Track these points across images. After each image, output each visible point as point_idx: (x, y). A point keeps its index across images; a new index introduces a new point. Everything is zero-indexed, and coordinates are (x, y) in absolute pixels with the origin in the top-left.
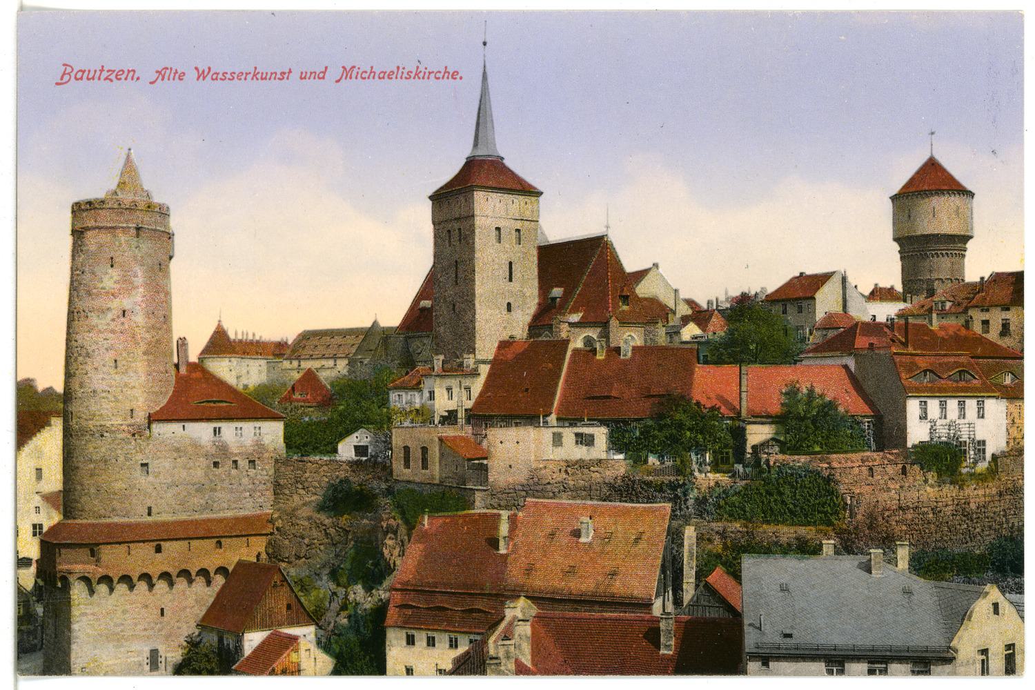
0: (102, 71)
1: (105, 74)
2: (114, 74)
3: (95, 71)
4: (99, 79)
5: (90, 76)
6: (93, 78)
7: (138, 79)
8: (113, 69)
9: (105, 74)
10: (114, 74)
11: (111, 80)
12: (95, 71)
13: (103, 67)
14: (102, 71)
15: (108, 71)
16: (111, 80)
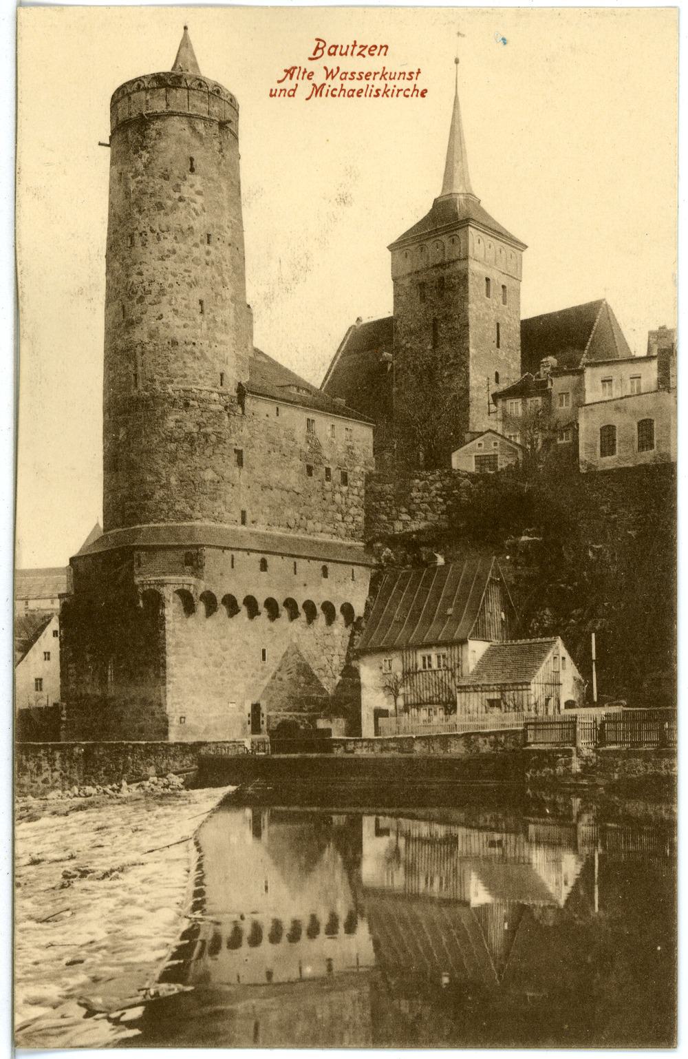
0: (354, 46)
1: (357, 50)
2: (367, 49)
3: (348, 46)
4: (352, 54)
5: (343, 52)
6: (346, 54)
8: (365, 45)
9: (357, 50)
10: (367, 49)
11: (364, 56)
12: (348, 46)
13: (355, 42)
14: (354, 46)
16: (364, 56)
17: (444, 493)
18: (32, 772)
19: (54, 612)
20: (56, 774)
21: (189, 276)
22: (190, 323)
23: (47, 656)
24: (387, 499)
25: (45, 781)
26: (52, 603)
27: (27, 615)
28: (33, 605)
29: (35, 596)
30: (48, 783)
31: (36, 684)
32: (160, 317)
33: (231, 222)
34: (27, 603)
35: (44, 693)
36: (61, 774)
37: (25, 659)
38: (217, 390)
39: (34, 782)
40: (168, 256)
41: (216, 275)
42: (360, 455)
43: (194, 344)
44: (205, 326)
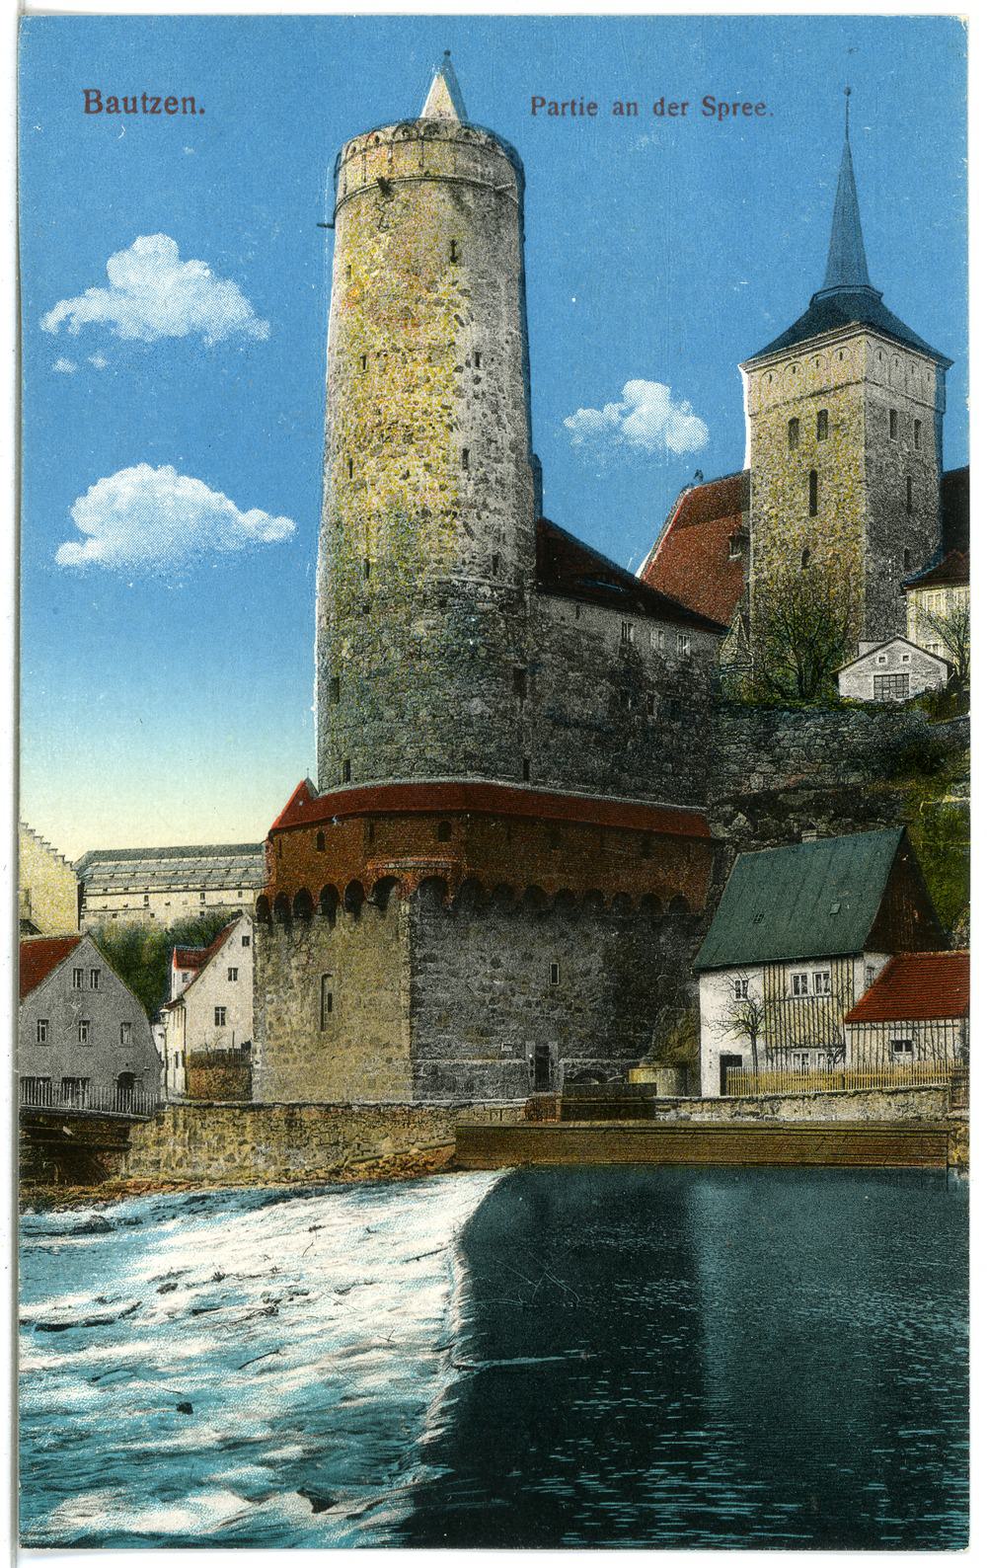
17: (828, 731)
18: (209, 1145)
19: (243, 909)
20: (247, 1148)
21: (450, 415)
22: (452, 484)
23: (233, 974)
24: (741, 741)
25: (230, 1158)
26: (240, 894)
27: (202, 913)
28: (213, 898)
29: (217, 886)
30: (235, 1161)
31: (217, 1015)
32: (406, 476)
33: (511, 334)
34: (203, 896)
35: (228, 1028)
36: (253, 1148)
37: (200, 979)
38: (488, 581)
39: (212, 1159)
40: (417, 386)
41: (489, 412)
42: (701, 674)
43: (455, 514)
44: (471, 488)
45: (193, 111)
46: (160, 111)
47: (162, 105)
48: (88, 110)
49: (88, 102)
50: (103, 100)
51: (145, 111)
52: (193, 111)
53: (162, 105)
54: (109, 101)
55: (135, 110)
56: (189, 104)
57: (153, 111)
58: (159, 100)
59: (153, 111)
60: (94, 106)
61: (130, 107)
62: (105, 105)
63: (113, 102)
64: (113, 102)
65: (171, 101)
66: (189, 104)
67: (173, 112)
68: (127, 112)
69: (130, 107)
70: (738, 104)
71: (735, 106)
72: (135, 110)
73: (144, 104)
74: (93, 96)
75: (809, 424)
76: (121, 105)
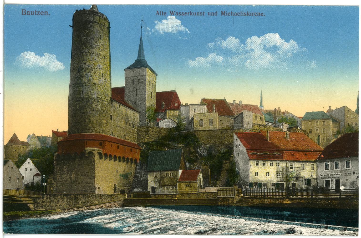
0: (36, 11)
7: (49, 15)
9: (37, 13)
15: (38, 12)
45: (47, 15)
46: (39, 15)
47: (40, 13)
48: (22, 14)
49: (23, 12)
50: (26, 12)
51: (36, 15)
52: (47, 15)
53: (40, 13)
54: (27, 12)
55: (33, 14)
56: (46, 13)
57: (38, 15)
58: (39, 12)
59: (38, 15)
60: (24, 13)
61: (32, 14)
62: (27, 13)
63: (28, 12)
64: (28, 12)
65: (42, 12)
66: (46, 13)
67: (43, 15)
68: (32, 15)
69: (32, 14)
70: (254, 13)
71: (253, 13)
72: (33, 14)
73: (36, 13)
74: (24, 11)
75: (136, 80)
76: (30, 13)
